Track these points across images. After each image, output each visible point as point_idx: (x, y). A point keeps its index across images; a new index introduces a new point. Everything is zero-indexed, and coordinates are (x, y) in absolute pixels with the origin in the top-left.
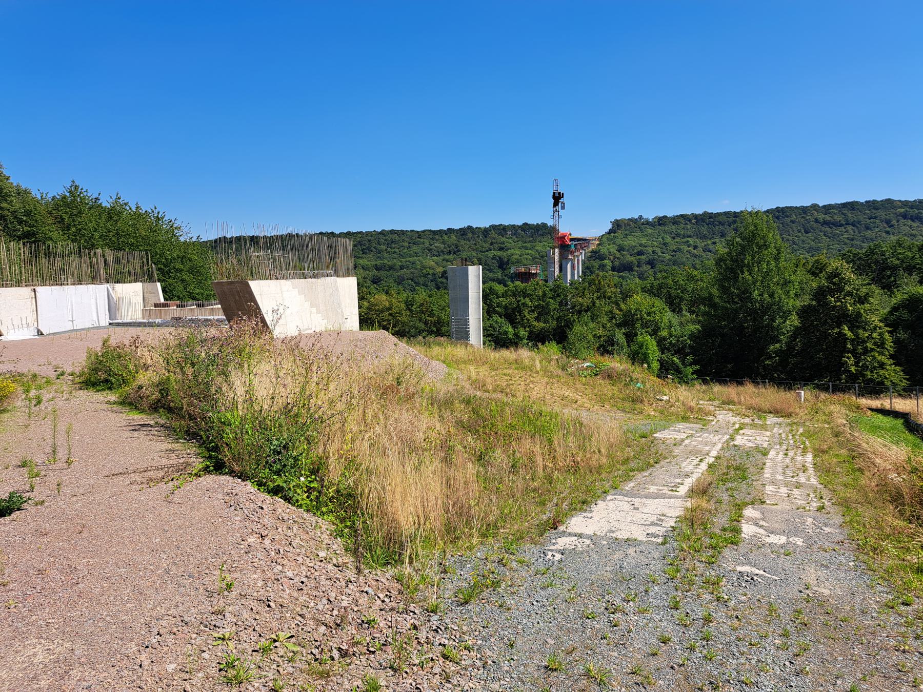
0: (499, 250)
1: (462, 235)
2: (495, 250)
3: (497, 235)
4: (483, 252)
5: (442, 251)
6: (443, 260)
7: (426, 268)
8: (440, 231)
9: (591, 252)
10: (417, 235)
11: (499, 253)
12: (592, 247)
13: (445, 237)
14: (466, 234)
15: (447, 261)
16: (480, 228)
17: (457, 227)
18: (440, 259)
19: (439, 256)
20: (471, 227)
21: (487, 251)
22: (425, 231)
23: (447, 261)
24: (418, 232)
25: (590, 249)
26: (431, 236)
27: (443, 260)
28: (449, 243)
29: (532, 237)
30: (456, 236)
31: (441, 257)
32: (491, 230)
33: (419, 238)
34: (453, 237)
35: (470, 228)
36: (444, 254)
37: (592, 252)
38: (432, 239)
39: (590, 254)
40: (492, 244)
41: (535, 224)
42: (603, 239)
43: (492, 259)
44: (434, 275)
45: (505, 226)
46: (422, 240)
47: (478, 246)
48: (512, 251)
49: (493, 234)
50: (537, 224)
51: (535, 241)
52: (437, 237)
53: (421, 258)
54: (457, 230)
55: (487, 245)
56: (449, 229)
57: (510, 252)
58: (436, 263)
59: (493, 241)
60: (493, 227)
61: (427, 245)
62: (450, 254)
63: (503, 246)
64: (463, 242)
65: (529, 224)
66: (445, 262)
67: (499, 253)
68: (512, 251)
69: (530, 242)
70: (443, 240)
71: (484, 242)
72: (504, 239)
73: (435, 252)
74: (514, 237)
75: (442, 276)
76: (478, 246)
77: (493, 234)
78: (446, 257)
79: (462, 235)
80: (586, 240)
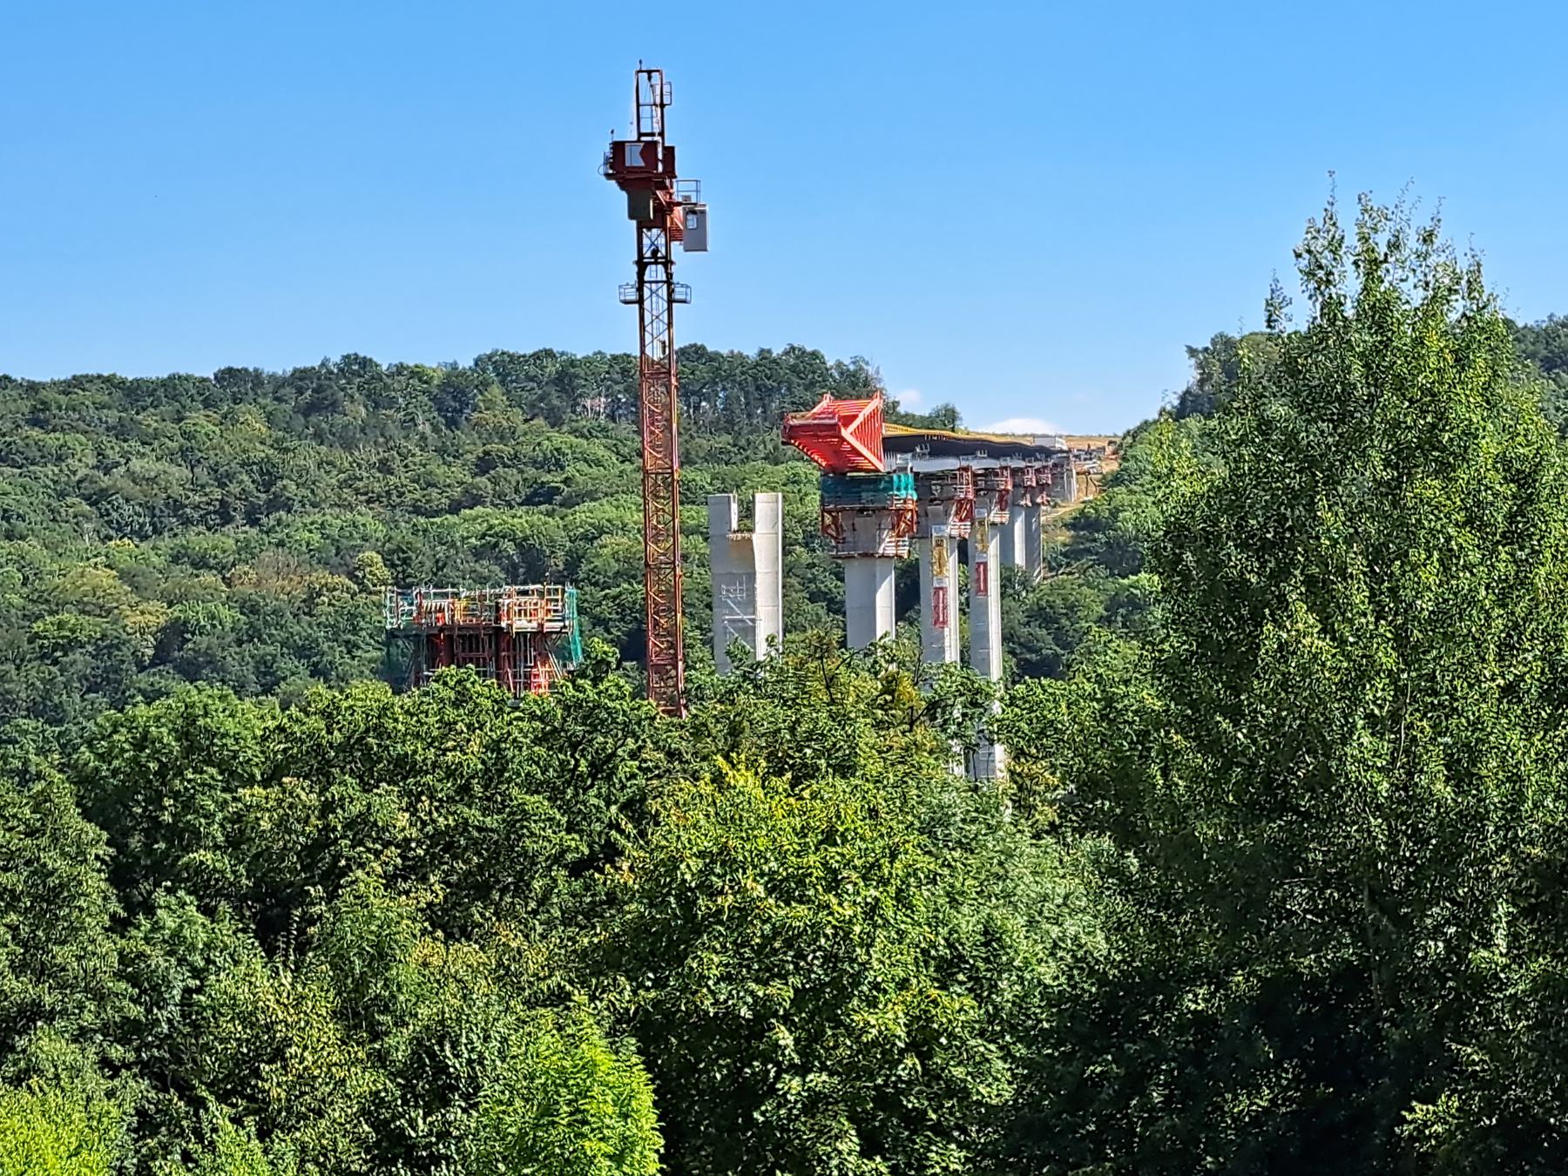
0: (527, 501)
1: (308, 410)
2: (500, 498)
3: (518, 416)
4: (430, 514)
5: (176, 506)
6: (176, 559)
7: (62, 605)
8: (172, 388)
9: (1074, 525)
10: (25, 406)
11: (523, 520)
12: (1079, 496)
13: (200, 420)
14: (334, 406)
15: (200, 563)
16: (417, 373)
17: (277, 362)
18: (153, 554)
19: (157, 532)
20: (365, 363)
21: (455, 508)
22: (78, 382)
23: (200, 563)
24: (33, 387)
25: (1068, 509)
26: (112, 416)
27: (176, 559)
28: (226, 457)
29: (729, 425)
30: (270, 418)
31: (166, 543)
32: (484, 385)
33: (35, 423)
34: (253, 421)
35: (358, 366)
36: (187, 522)
37: (1083, 523)
38: (120, 432)
39: (1064, 537)
40: (484, 465)
41: (751, 353)
42: (1139, 450)
43: (478, 554)
44: (107, 647)
45: (572, 363)
46: (52, 440)
47: (400, 478)
48: (603, 511)
49: (495, 406)
50: (764, 354)
51: (743, 450)
52: (149, 420)
53: (32, 548)
54: (279, 383)
55: (457, 474)
56: (229, 376)
57: (583, 514)
58: (125, 576)
59: (494, 447)
60: (503, 367)
61: (82, 464)
62: (227, 519)
63: (553, 479)
64: (307, 455)
65: (715, 357)
66: (181, 572)
67: (523, 520)
68: (603, 511)
69: (712, 457)
70: (188, 436)
71: (441, 451)
72: (561, 439)
73: (127, 510)
74: (625, 428)
75: (161, 657)
76: (400, 478)
77: (495, 406)
78: (199, 540)
79: (308, 410)
80: (1047, 452)
